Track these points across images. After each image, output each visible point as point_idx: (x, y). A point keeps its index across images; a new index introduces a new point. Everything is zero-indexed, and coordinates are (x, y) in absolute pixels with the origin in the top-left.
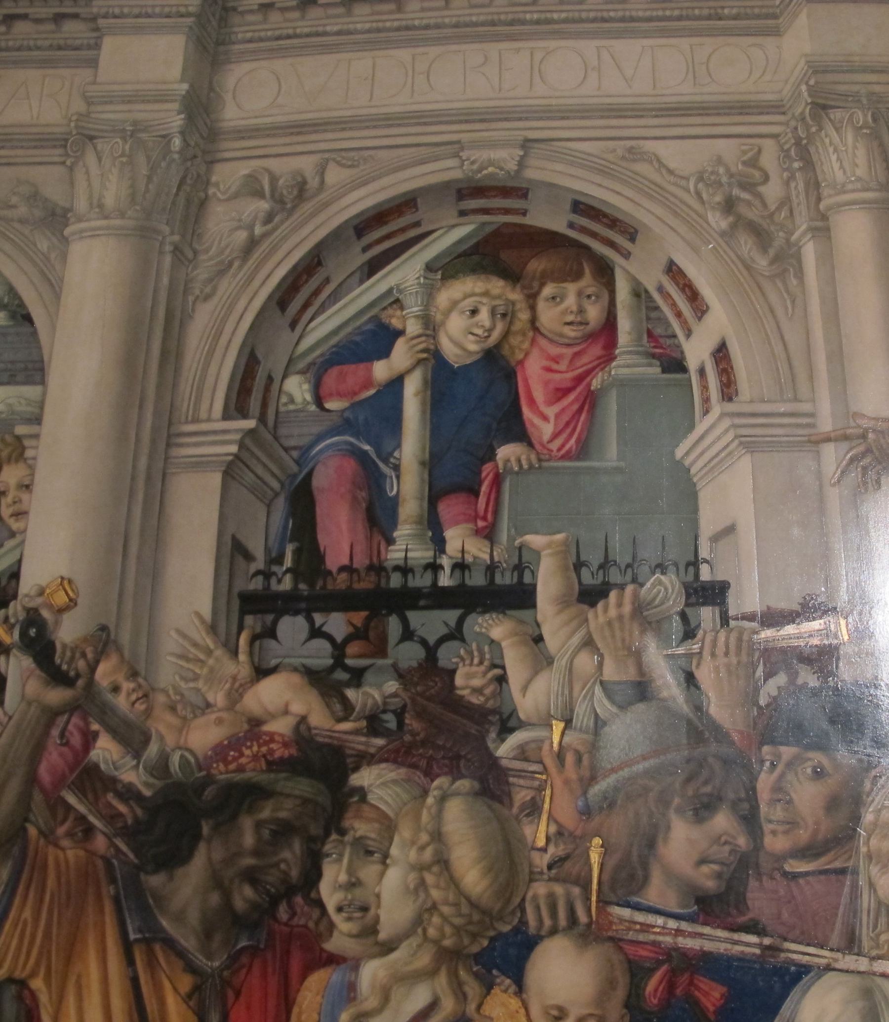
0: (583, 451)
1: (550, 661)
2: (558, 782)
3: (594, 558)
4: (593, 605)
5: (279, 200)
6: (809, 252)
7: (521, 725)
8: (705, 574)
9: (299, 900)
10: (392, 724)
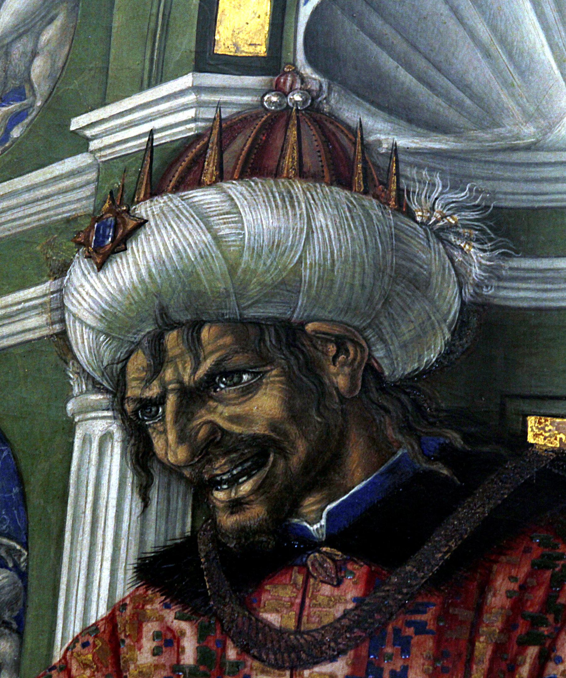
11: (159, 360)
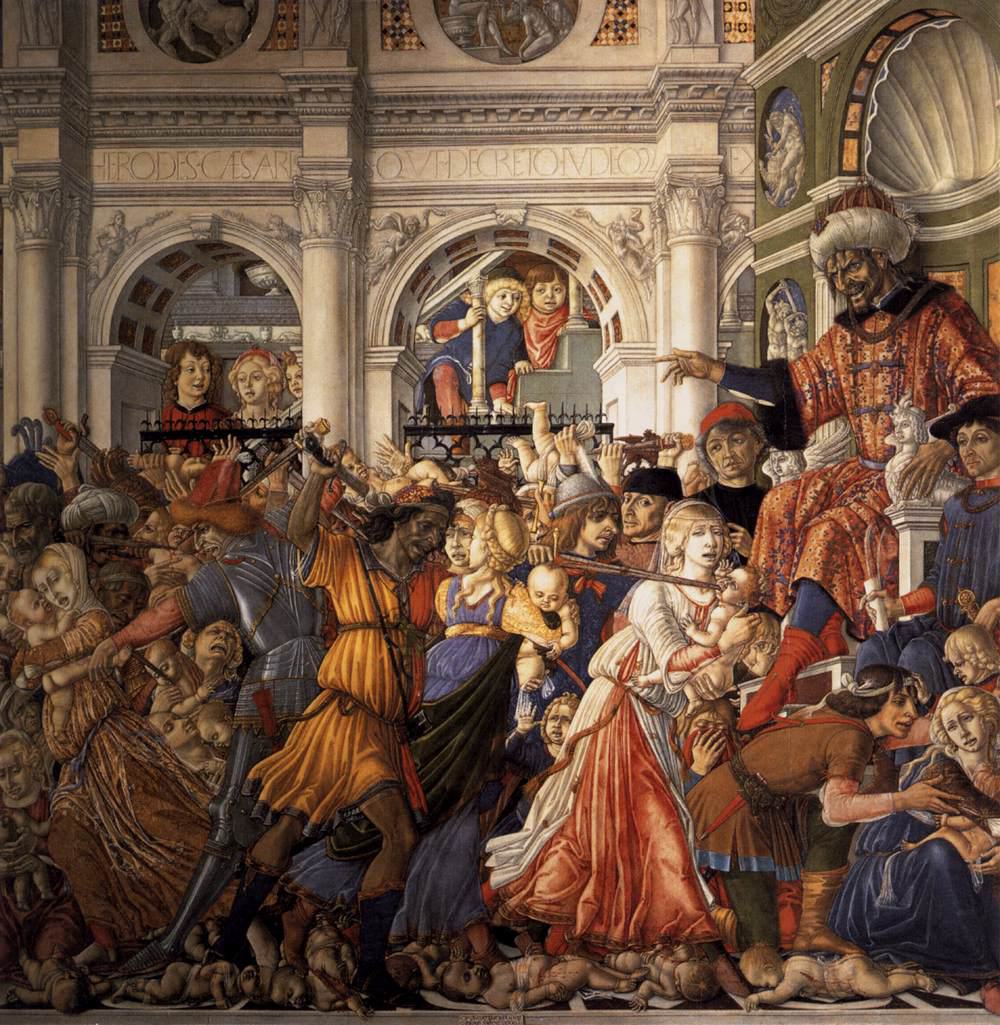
0: (553, 365)
1: (538, 457)
2: (540, 504)
3: (558, 415)
4: (556, 433)
5: (406, 232)
6: (660, 267)
7: (528, 483)
8: (604, 421)
9: (437, 553)
10: (474, 483)
11: (835, 261)
